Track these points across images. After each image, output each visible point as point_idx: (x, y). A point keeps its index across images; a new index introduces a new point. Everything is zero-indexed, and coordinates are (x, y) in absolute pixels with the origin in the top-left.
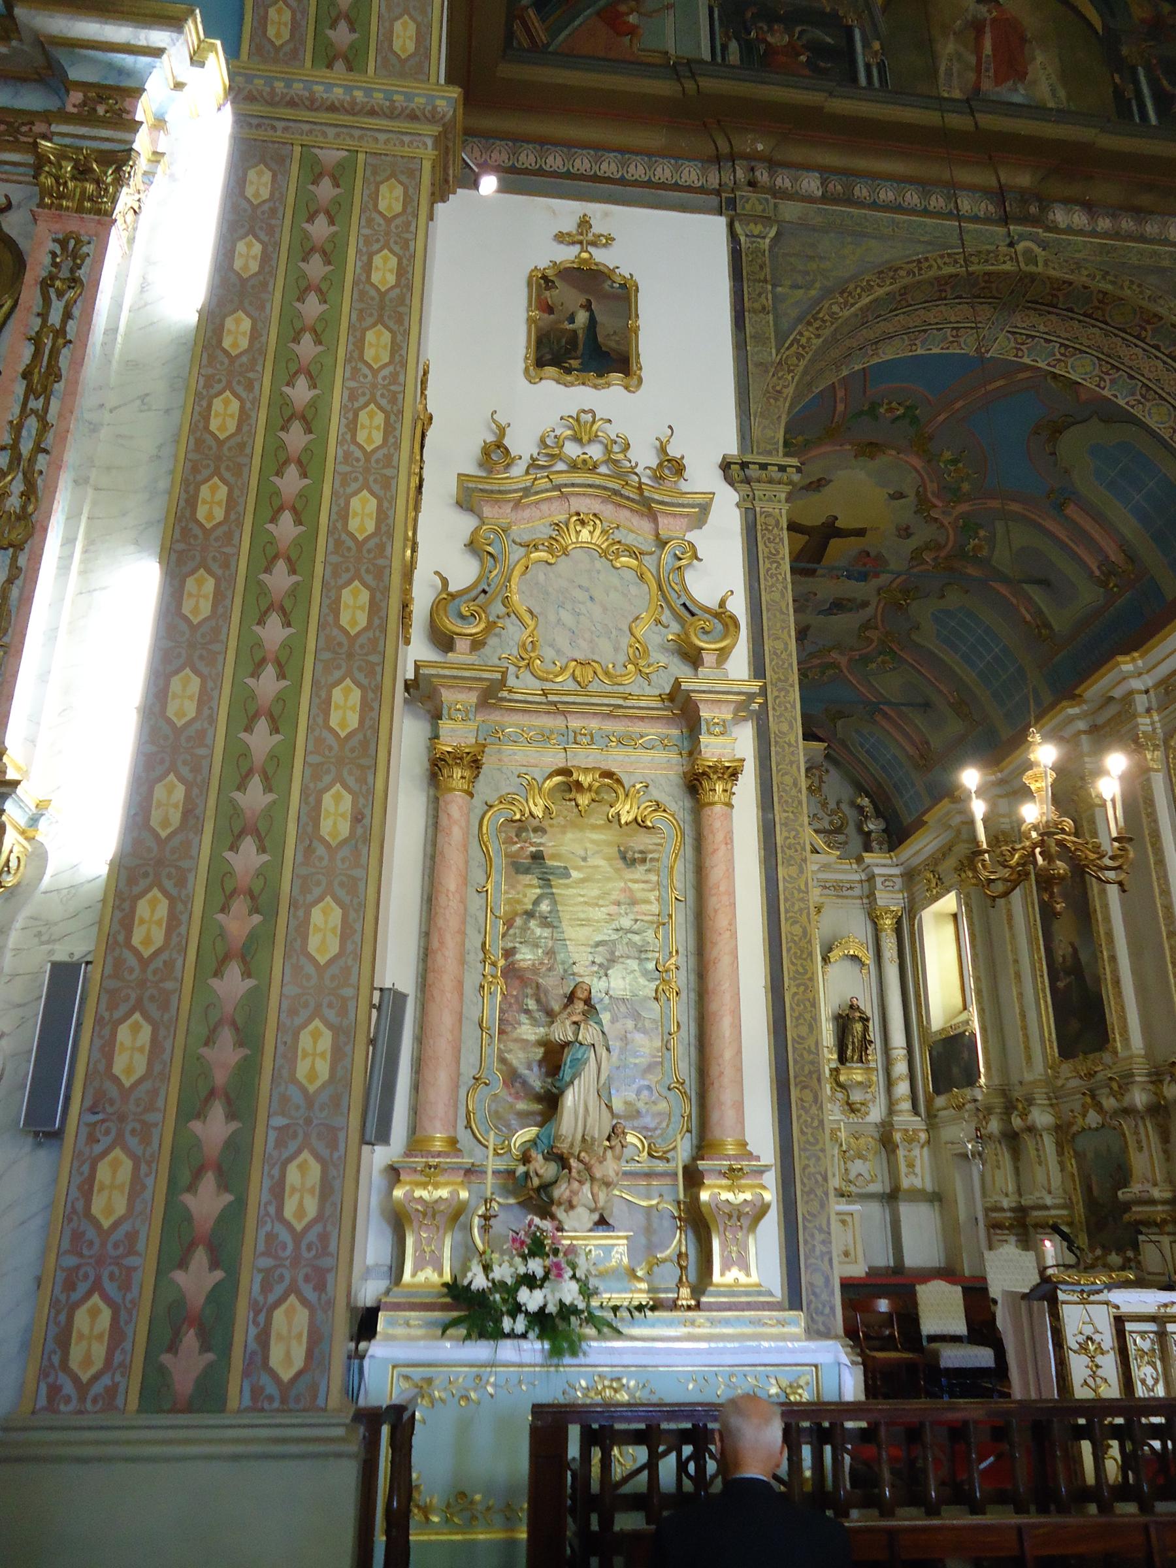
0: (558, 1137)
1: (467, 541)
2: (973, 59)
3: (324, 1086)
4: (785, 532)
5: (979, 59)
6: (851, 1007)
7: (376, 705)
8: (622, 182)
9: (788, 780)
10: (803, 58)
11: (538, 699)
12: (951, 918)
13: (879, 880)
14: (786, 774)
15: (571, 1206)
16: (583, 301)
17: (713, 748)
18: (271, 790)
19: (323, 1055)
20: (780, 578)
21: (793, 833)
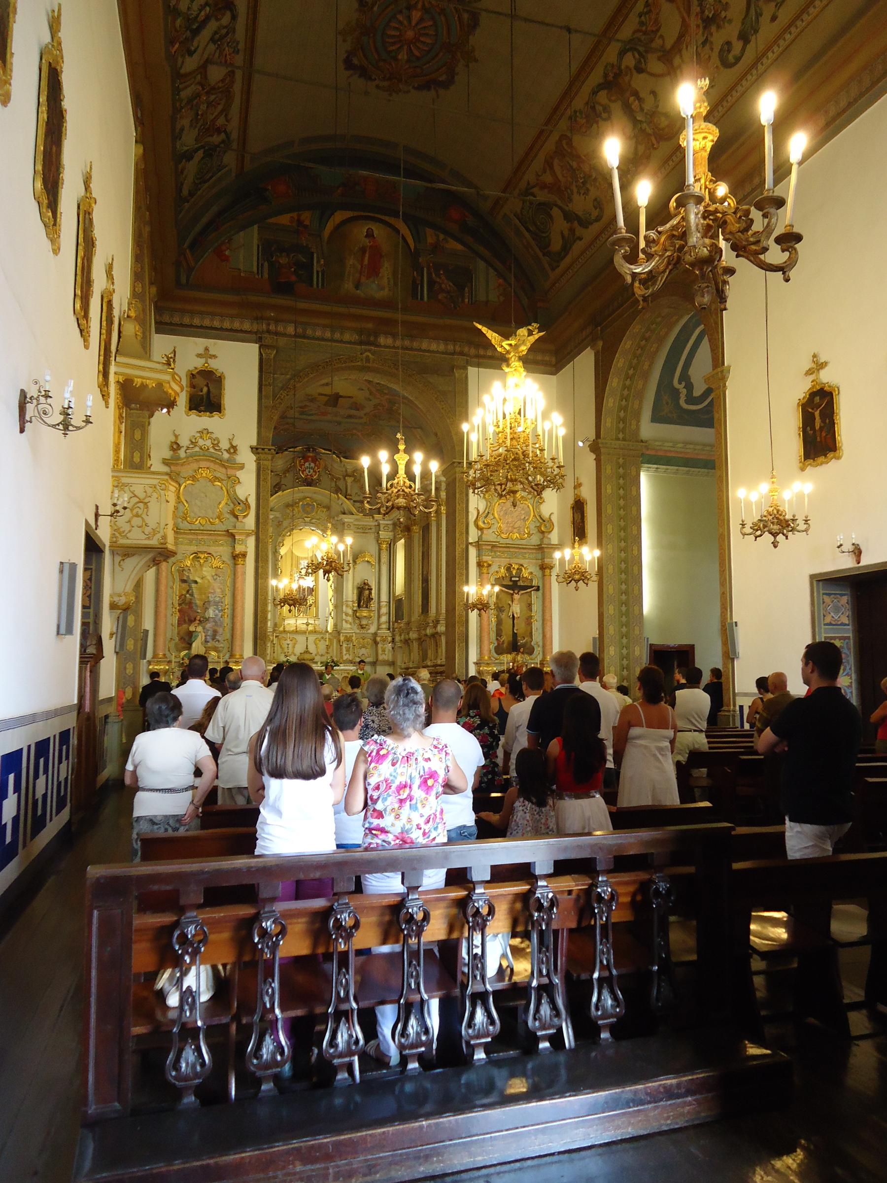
2: (359, 267)
5: (362, 267)
6: (365, 583)
8: (221, 329)
10: (293, 269)
17: (239, 549)
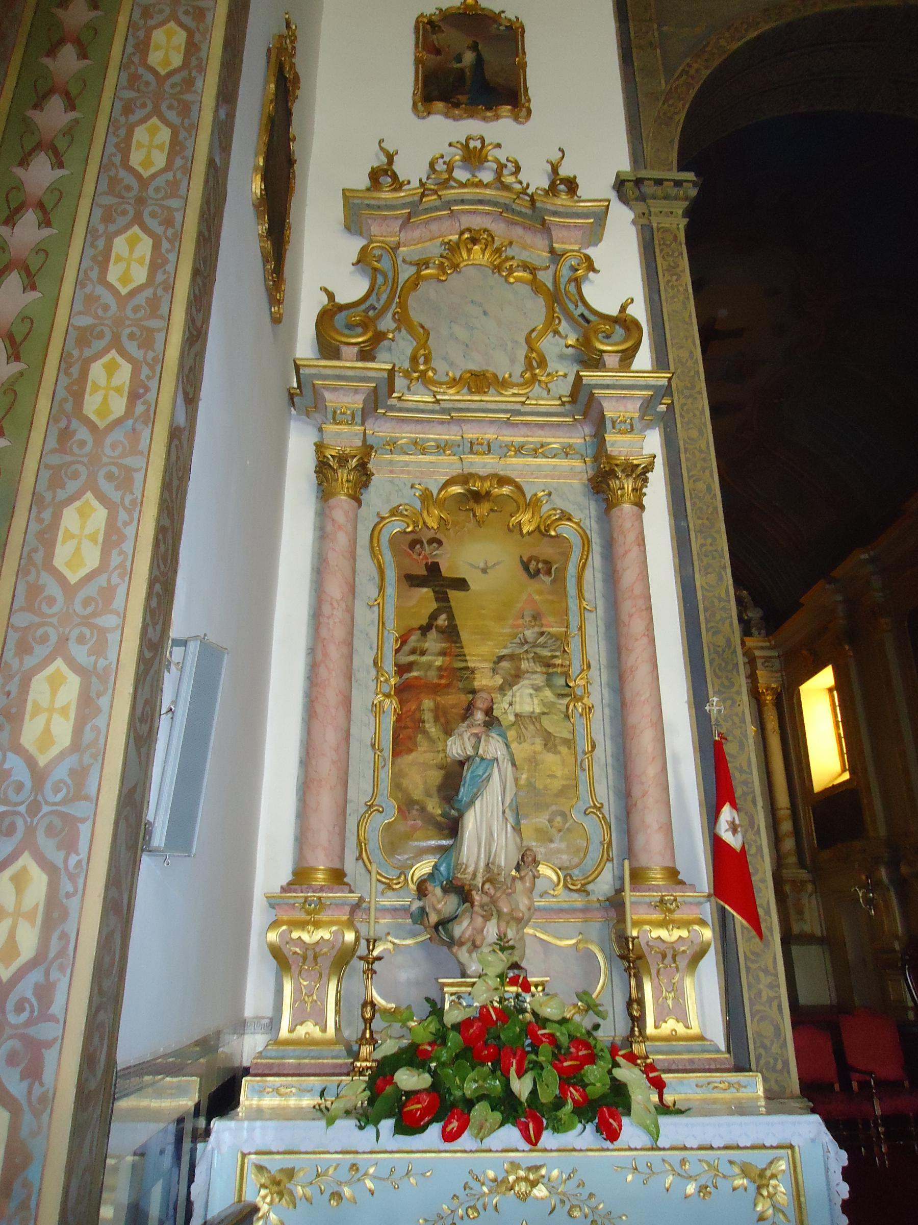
0: (458, 866)
1: (355, 261)
3: (62, 755)
4: (684, 246)
7: (172, 257)
9: (701, 486)
11: (430, 406)
12: (827, 691)
13: (759, 662)
14: (699, 480)
15: (475, 946)
16: (469, 41)
18: (17, 358)
19: (64, 711)
20: (681, 289)
21: (709, 541)
